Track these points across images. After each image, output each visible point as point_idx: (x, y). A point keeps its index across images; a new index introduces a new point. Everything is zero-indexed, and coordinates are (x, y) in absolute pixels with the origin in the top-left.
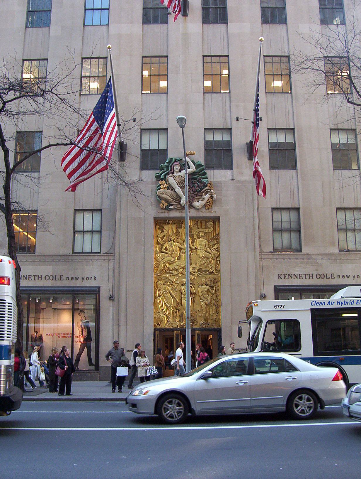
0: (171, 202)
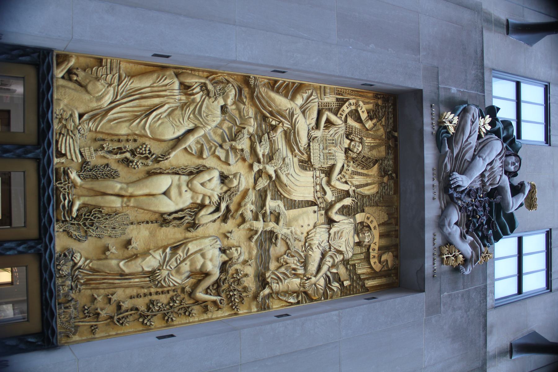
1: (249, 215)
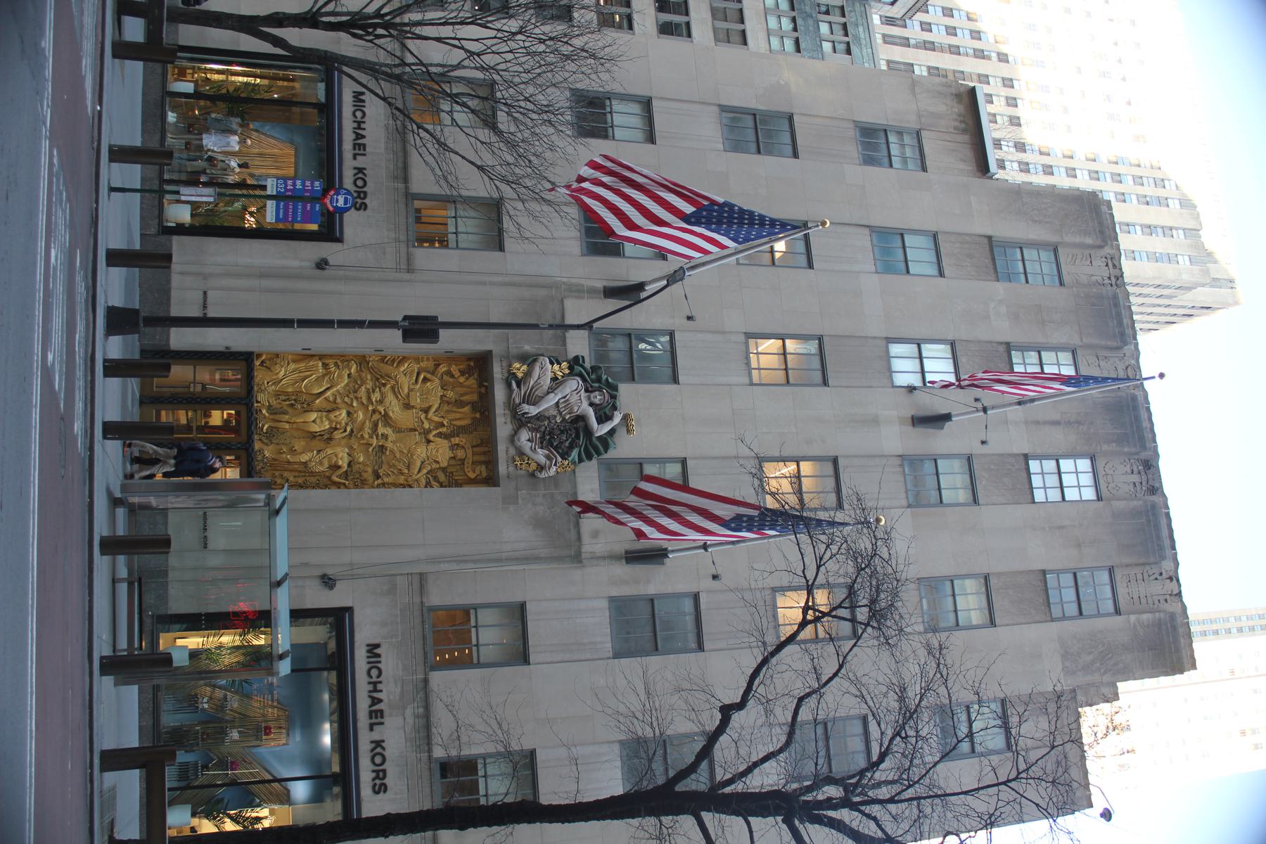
0: (525, 383)
1: (366, 436)
